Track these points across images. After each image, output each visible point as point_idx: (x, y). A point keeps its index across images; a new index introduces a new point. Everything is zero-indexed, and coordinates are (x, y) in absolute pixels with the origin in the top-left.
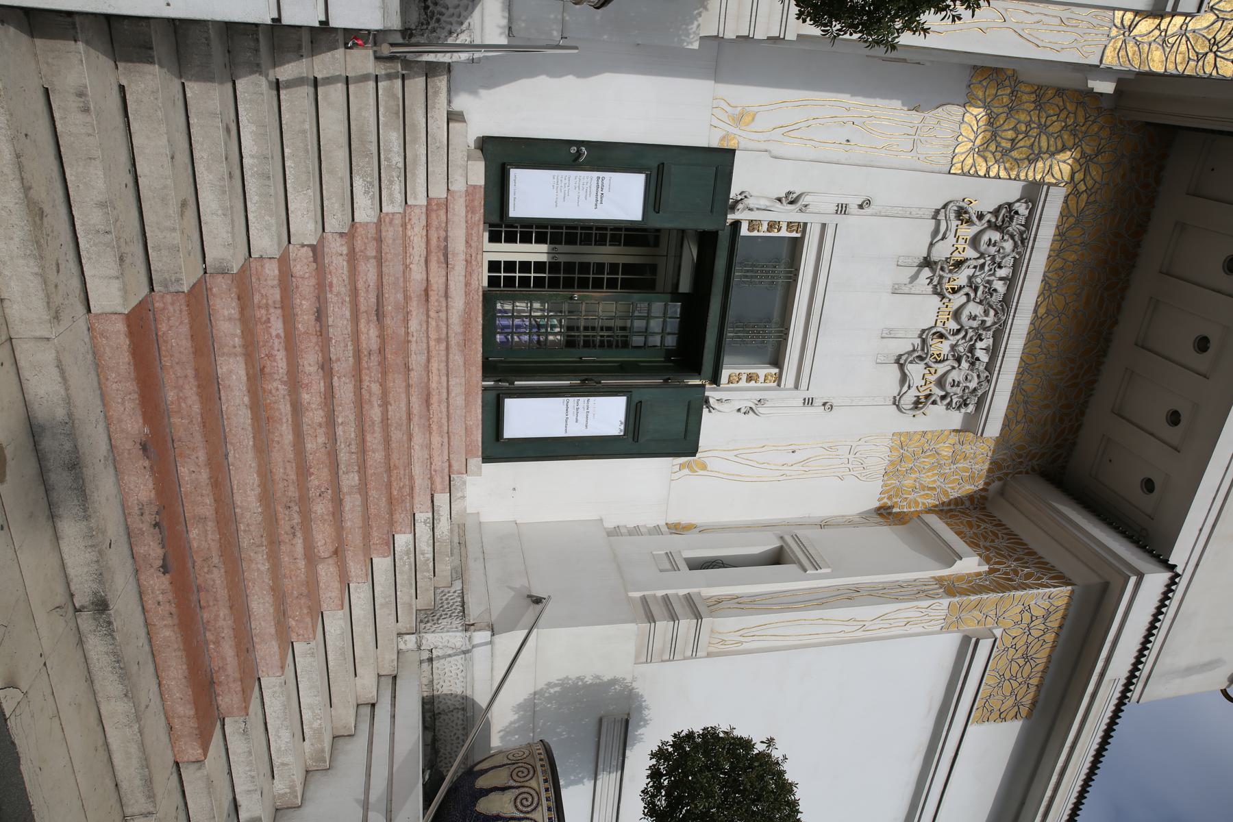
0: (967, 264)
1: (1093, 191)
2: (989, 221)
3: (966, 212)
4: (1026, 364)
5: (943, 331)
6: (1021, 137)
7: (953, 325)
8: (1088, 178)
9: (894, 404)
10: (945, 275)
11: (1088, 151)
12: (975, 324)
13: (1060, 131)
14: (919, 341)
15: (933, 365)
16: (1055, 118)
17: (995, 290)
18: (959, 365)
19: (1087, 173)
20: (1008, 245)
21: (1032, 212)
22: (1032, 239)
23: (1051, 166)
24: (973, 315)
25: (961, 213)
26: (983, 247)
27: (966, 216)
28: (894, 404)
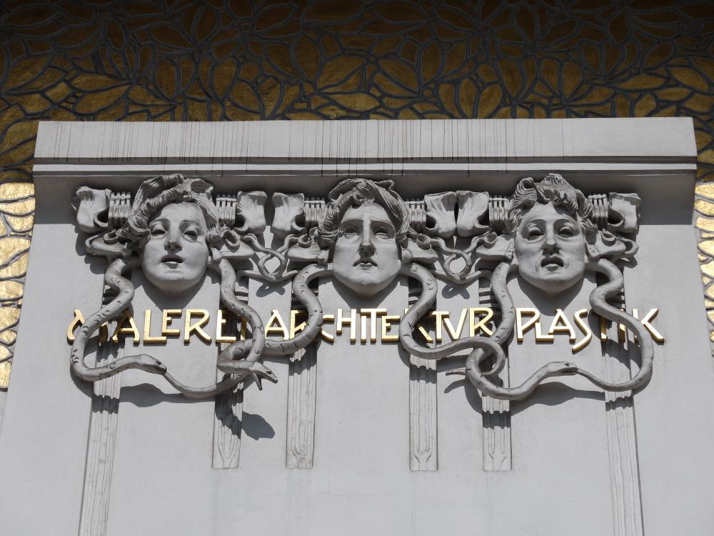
0: (230, 300)
2: (126, 274)
3: (104, 331)
4: (503, 104)
5: (411, 318)
7: (399, 301)
8: (38, 84)
12: (384, 246)
15: (505, 323)
17: (300, 220)
18: (505, 259)
20: (175, 214)
21: (97, 183)
26: (185, 272)
27: (112, 327)
28: (628, 402)
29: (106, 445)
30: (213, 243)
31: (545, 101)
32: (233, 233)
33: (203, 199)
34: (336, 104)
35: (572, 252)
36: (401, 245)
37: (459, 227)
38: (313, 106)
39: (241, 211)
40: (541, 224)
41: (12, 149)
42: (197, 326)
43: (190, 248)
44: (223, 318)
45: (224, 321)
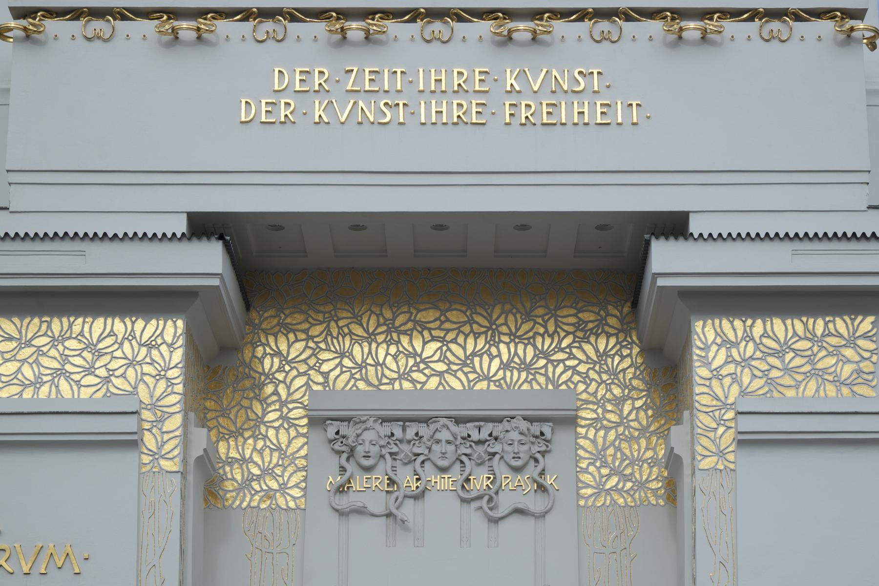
6: (268, 443)
9: (544, 516)
13: (260, 402)
15: (498, 484)
16: (249, 411)
17: (417, 434)
18: (496, 453)
24: (441, 455)
25: (341, 490)
31: (518, 367)
32: (390, 441)
33: (377, 426)
34: (428, 367)
40: (512, 440)
42: (377, 484)
45: (388, 482)
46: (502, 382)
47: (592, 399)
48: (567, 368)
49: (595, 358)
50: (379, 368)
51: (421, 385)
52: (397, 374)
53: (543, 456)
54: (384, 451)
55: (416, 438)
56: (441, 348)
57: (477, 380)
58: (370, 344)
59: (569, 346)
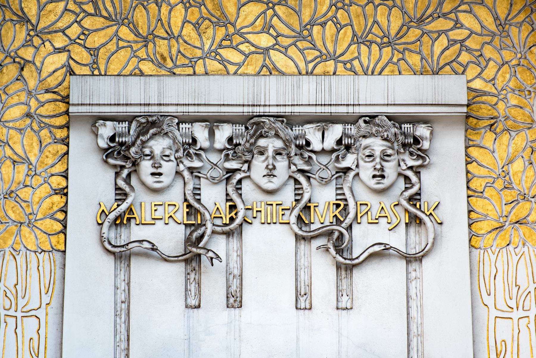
1: (78, 10)
6: (9, 152)
8: (60, 25)
9: (421, 261)
10: (209, 232)
11: (22, 34)
14: (316, 243)
15: (351, 216)
17: (230, 140)
19: (54, 28)
22: (147, 109)
23: (47, 91)
29: (124, 291)
30: (179, 160)
31: (379, 40)
33: (174, 129)
34: (248, 42)
35: (390, 168)
36: (290, 163)
37: (325, 148)
38: (234, 44)
39: (193, 134)
41: (49, 76)
42: (172, 214)
43: (168, 168)
44: (187, 208)
46: (356, 63)
47: (489, 88)
48: (452, 42)
49: (493, 28)
50: (173, 41)
51: (236, 68)
52: (201, 51)
53: (418, 174)
54: (181, 167)
55: (230, 147)
56: (264, 13)
57: (319, 59)
58: (160, 7)
59: (455, 10)
